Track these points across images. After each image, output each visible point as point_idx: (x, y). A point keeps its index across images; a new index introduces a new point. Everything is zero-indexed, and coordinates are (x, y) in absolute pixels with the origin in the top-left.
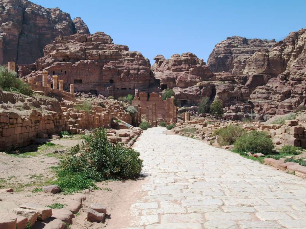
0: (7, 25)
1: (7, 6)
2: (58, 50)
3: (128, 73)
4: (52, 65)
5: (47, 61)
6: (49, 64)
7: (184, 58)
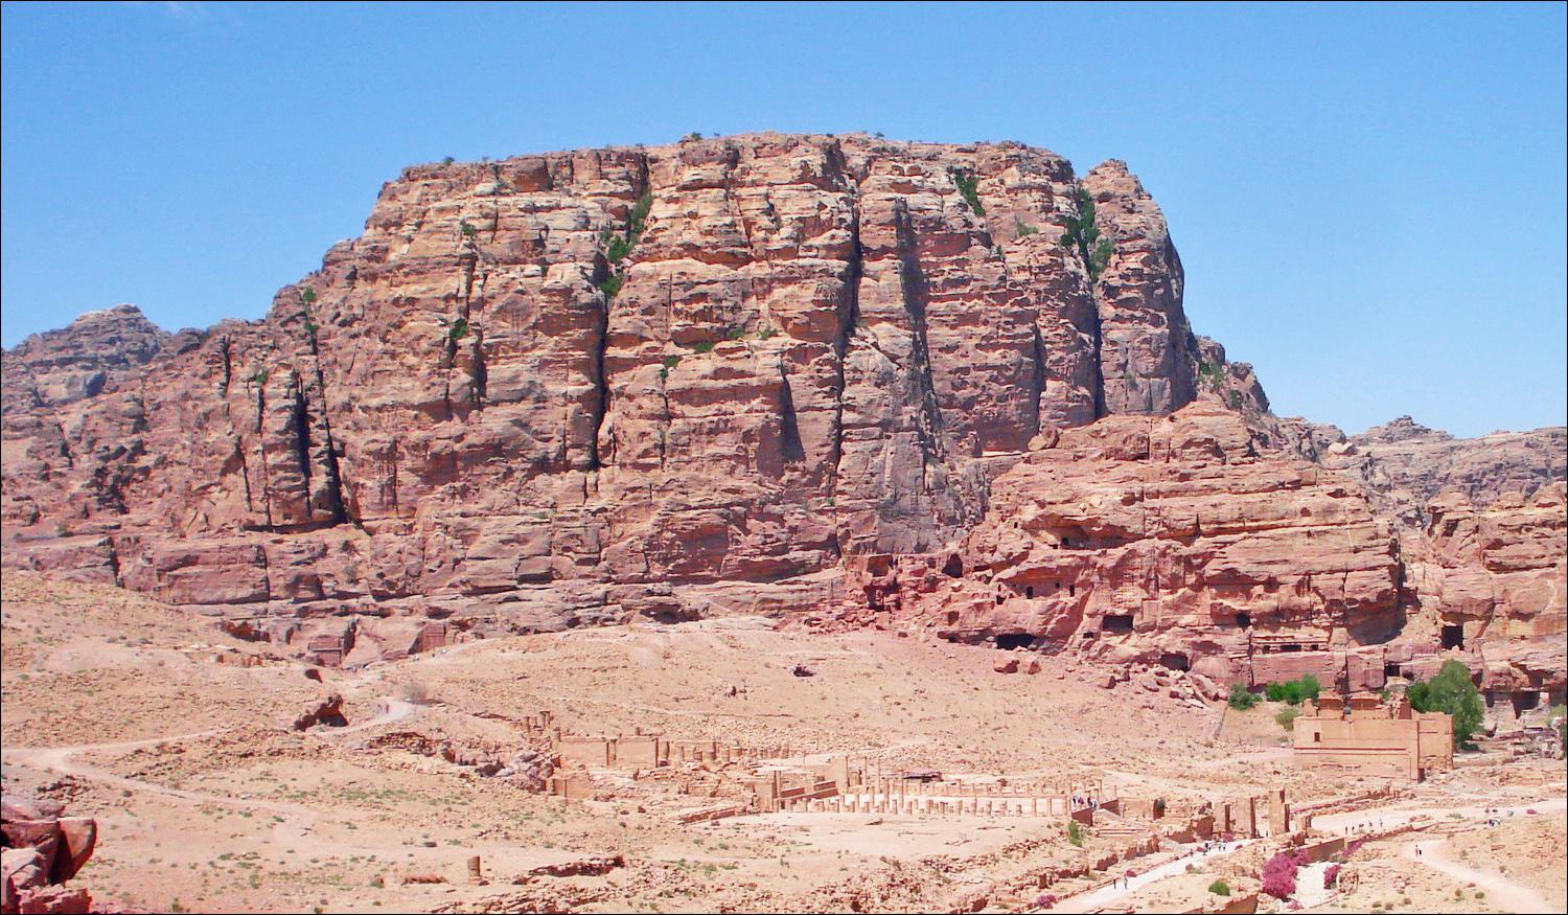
0: (792, 296)
1: (788, 203)
2: (1042, 505)
3: (1303, 586)
4: (1024, 566)
5: (1005, 549)
6: (1011, 560)
7: (1540, 511)
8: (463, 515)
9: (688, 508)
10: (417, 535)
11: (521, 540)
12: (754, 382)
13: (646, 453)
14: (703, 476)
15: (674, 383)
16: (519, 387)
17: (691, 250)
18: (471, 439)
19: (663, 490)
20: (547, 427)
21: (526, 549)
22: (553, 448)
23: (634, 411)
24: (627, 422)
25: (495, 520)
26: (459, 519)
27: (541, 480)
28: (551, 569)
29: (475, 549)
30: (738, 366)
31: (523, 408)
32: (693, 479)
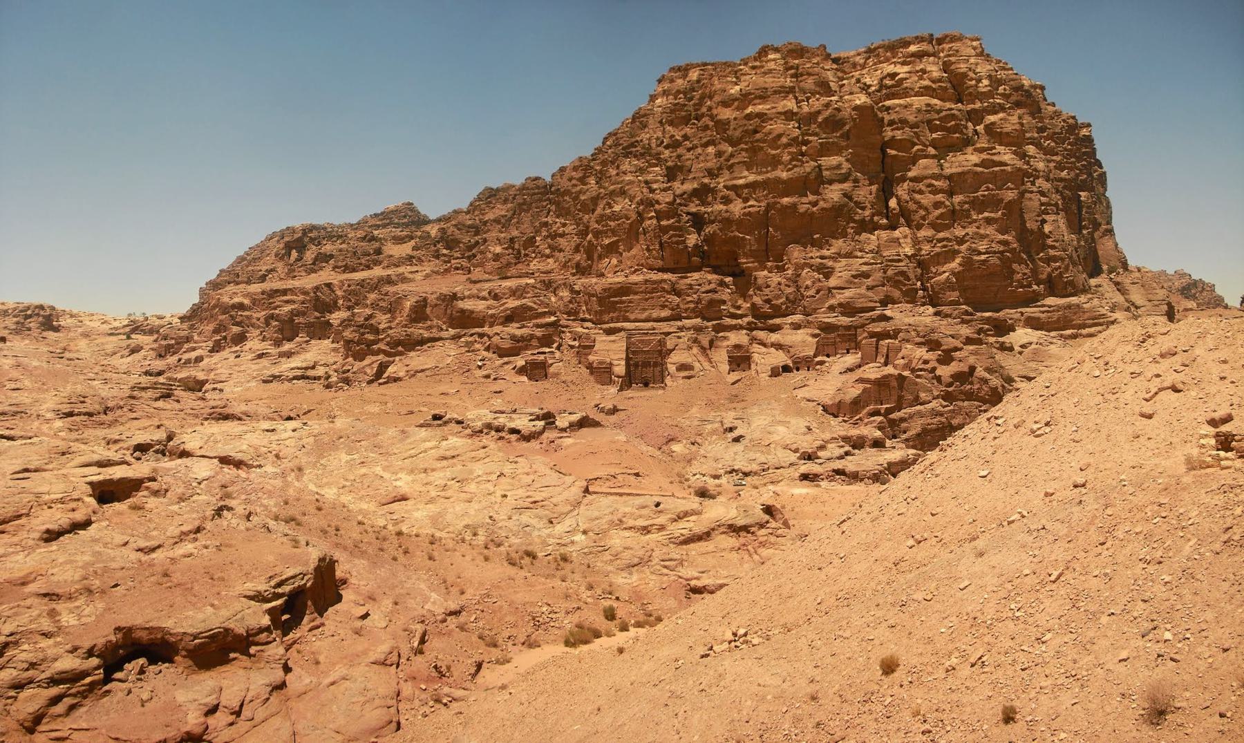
8: (822, 257)
9: (980, 253)
10: (790, 272)
11: (866, 275)
12: (1009, 168)
13: (941, 216)
14: (982, 231)
15: (948, 171)
16: (843, 171)
17: (926, 91)
18: (822, 204)
19: (961, 241)
20: (861, 199)
21: (869, 282)
22: (867, 213)
23: (924, 188)
24: (917, 196)
25: (844, 261)
26: (819, 260)
27: (864, 236)
28: (887, 296)
29: (833, 282)
30: (996, 158)
31: (847, 186)
32: (977, 233)
